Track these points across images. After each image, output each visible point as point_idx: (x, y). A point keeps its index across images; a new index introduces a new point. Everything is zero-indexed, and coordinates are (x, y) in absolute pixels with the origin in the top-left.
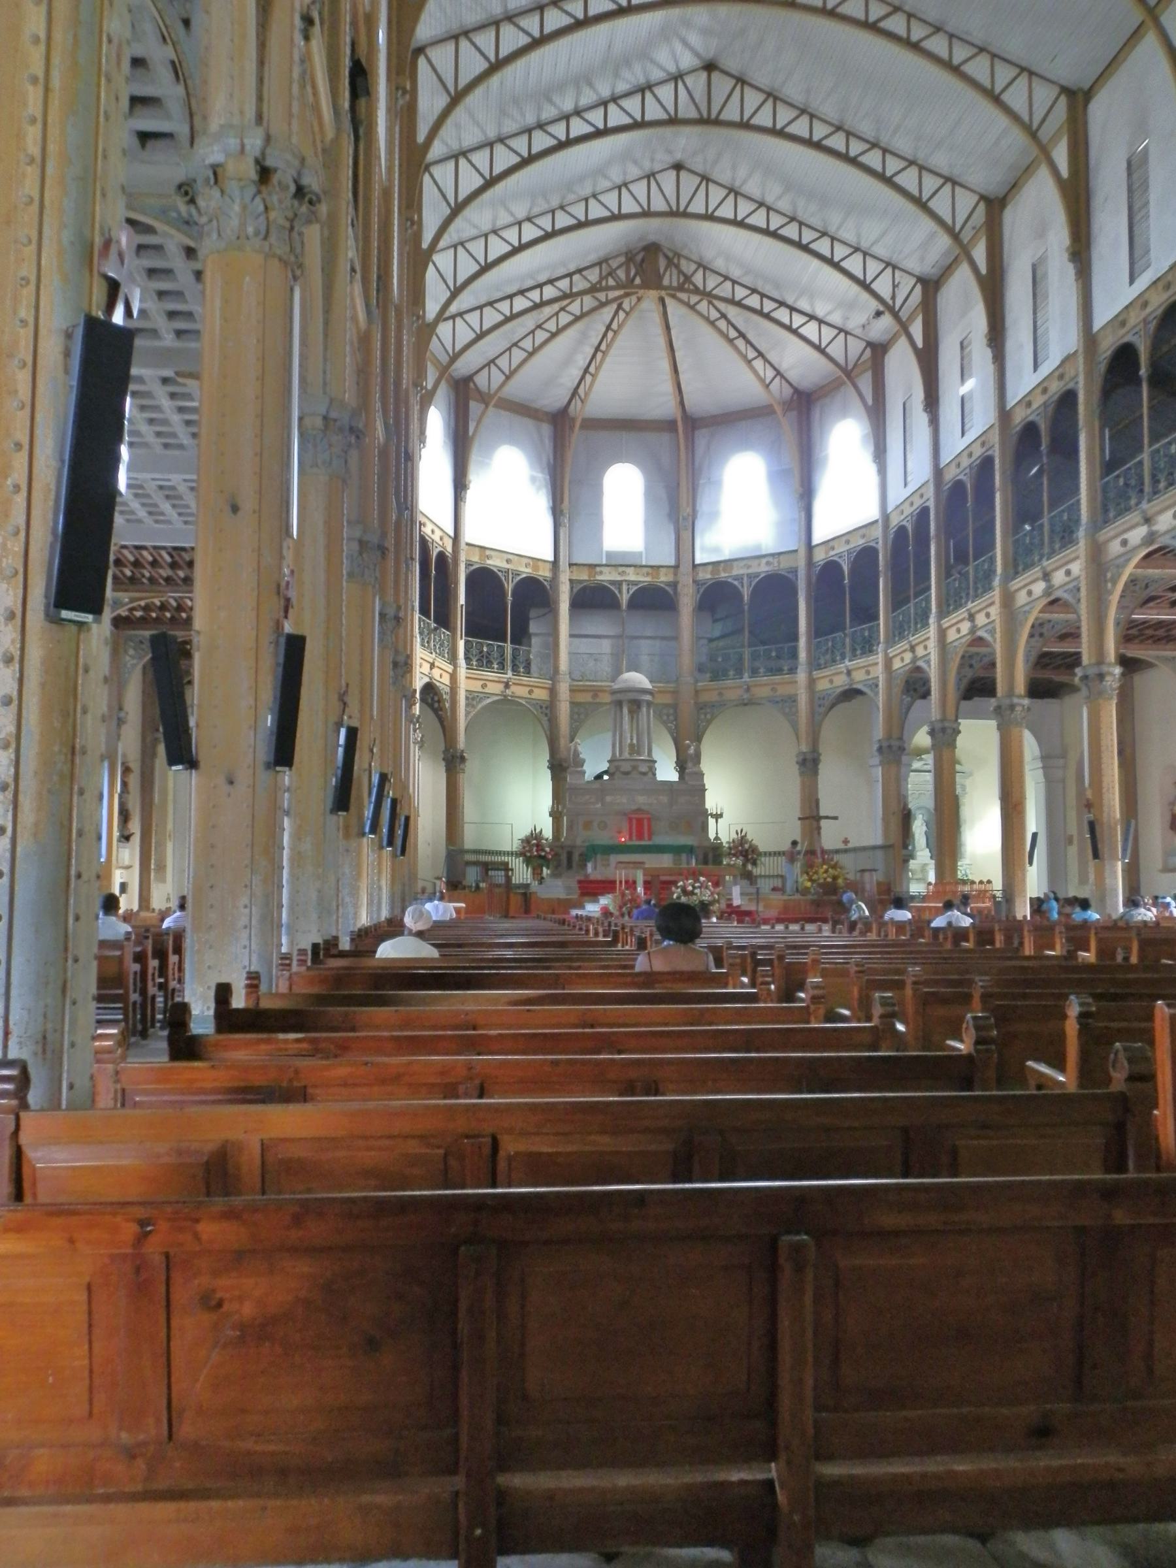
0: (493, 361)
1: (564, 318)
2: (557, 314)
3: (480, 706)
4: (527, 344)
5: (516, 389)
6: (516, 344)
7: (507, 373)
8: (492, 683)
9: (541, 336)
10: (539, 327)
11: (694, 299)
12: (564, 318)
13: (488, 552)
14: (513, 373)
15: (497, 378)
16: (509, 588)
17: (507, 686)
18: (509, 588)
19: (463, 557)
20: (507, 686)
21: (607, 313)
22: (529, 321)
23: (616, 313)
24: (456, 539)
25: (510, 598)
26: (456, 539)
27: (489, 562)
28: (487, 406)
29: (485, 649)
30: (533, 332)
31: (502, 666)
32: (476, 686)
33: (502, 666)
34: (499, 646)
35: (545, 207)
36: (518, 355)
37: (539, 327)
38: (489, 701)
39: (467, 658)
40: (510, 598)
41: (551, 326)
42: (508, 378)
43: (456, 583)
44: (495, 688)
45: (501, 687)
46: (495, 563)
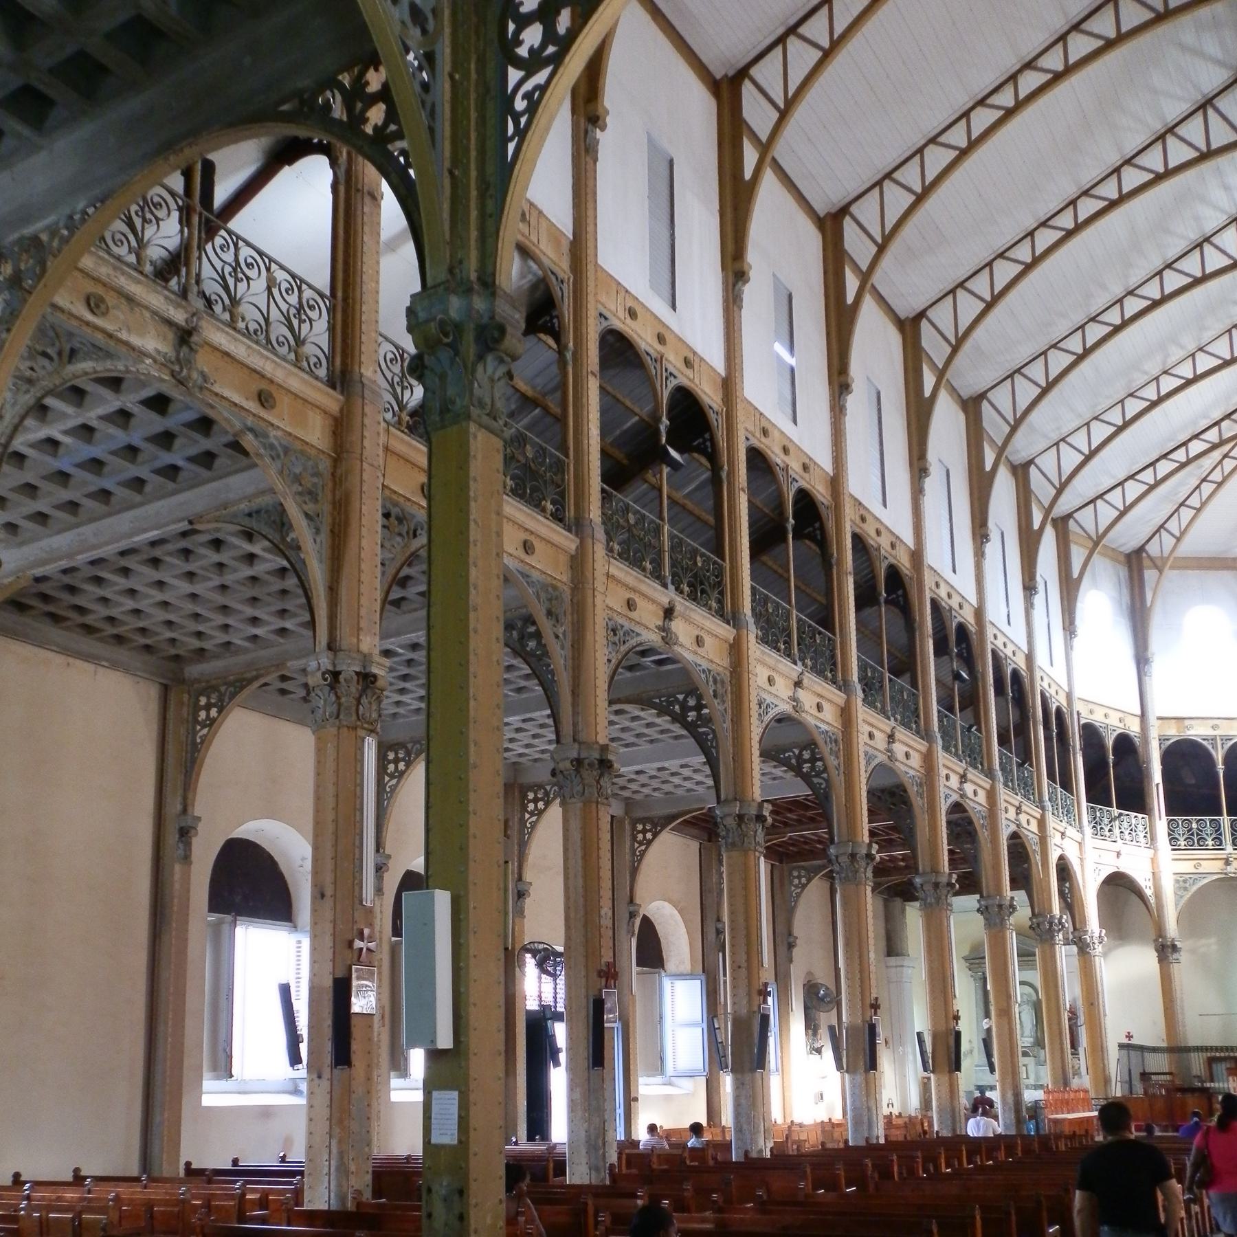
0: (1162, 526)
2: (1220, 462)
3: (1195, 888)
4: (1195, 501)
5: (1188, 547)
6: (1182, 504)
7: (1178, 534)
8: (1209, 863)
9: (1207, 488)
10: (1204, 480)
13: (1187, 723)
14: (1183, 533)
15: (1168, 541)
16: (1219, 757)
17: (1227, 862)
18: (1219, 757)
19: (1154, 734)
20: (1227, 862)
22: (1189, 478)
24: (1143, 716)
25: (1220, 768)
26: (1143, 716)
27: (1189, 733)
28: (1161, 571)
29: (1194, 826)
30: (1198, 487)
31: (1219, 840)
32: (1187, 867)
33: (1219, 840)
34: (1211, 821)
36: (1186, 514)
37: (1204, 480)
38: (1206, 881)
39: (1172, 839)
40: (1220, 768)
41: (1217, 476)
42: (1178, 539)
43: (1149, 762)
44: (1217, 866)
45: (1220, 864)
46: (1197, 732)
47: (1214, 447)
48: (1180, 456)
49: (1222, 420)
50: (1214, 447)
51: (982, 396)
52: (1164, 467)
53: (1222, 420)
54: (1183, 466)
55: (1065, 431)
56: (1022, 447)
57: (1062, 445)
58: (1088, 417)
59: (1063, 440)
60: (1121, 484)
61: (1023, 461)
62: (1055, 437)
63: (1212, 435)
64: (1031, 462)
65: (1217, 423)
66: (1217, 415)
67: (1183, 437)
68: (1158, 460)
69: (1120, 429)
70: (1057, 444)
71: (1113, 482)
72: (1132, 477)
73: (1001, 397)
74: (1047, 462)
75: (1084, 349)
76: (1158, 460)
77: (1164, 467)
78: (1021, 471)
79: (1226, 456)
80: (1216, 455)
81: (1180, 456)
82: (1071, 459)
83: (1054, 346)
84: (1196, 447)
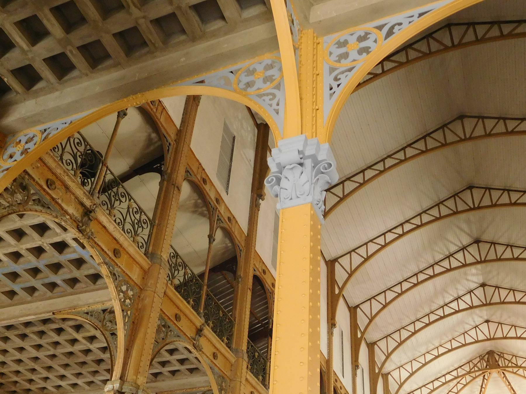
1: (460, 386)
2: (456, 385)
11: (515, 370)
12: (460, 386)
21: (479, 380)
23: (483, 381)
35: (447, 339)
47: (456, 378)
48: (443, 380)
49: (458, 368)
50: (456, 378)
51: (375, 343)
52: (437, 384)
53: (458, 368)
54: (444, 384)
55: (403, 363)
56: (388, 367)
57: (401, 368)
58: (411, 359)
59: (402, 366)
60: (420, 388)
61: (386, 373)
62: (399, 365)
63: (455, 373)
64: (389, 373)
65: (456, 369)
66: (456, 366)
67: (444, 372)
68: (434, 381)
69: (424, 365)
70: (399, 368)
71: (417, 387)
72: (424, 386)
73: (382, 344)
74: (395, 374)
75: (415, 331)
76: (434, 381)
77: (437, 384)
78: (385, 376)
79: (458, 383)
80: (455, 382)
81: (443, 380)
82: (405, 375)
83: (403, 328)
84: (449, 377)
